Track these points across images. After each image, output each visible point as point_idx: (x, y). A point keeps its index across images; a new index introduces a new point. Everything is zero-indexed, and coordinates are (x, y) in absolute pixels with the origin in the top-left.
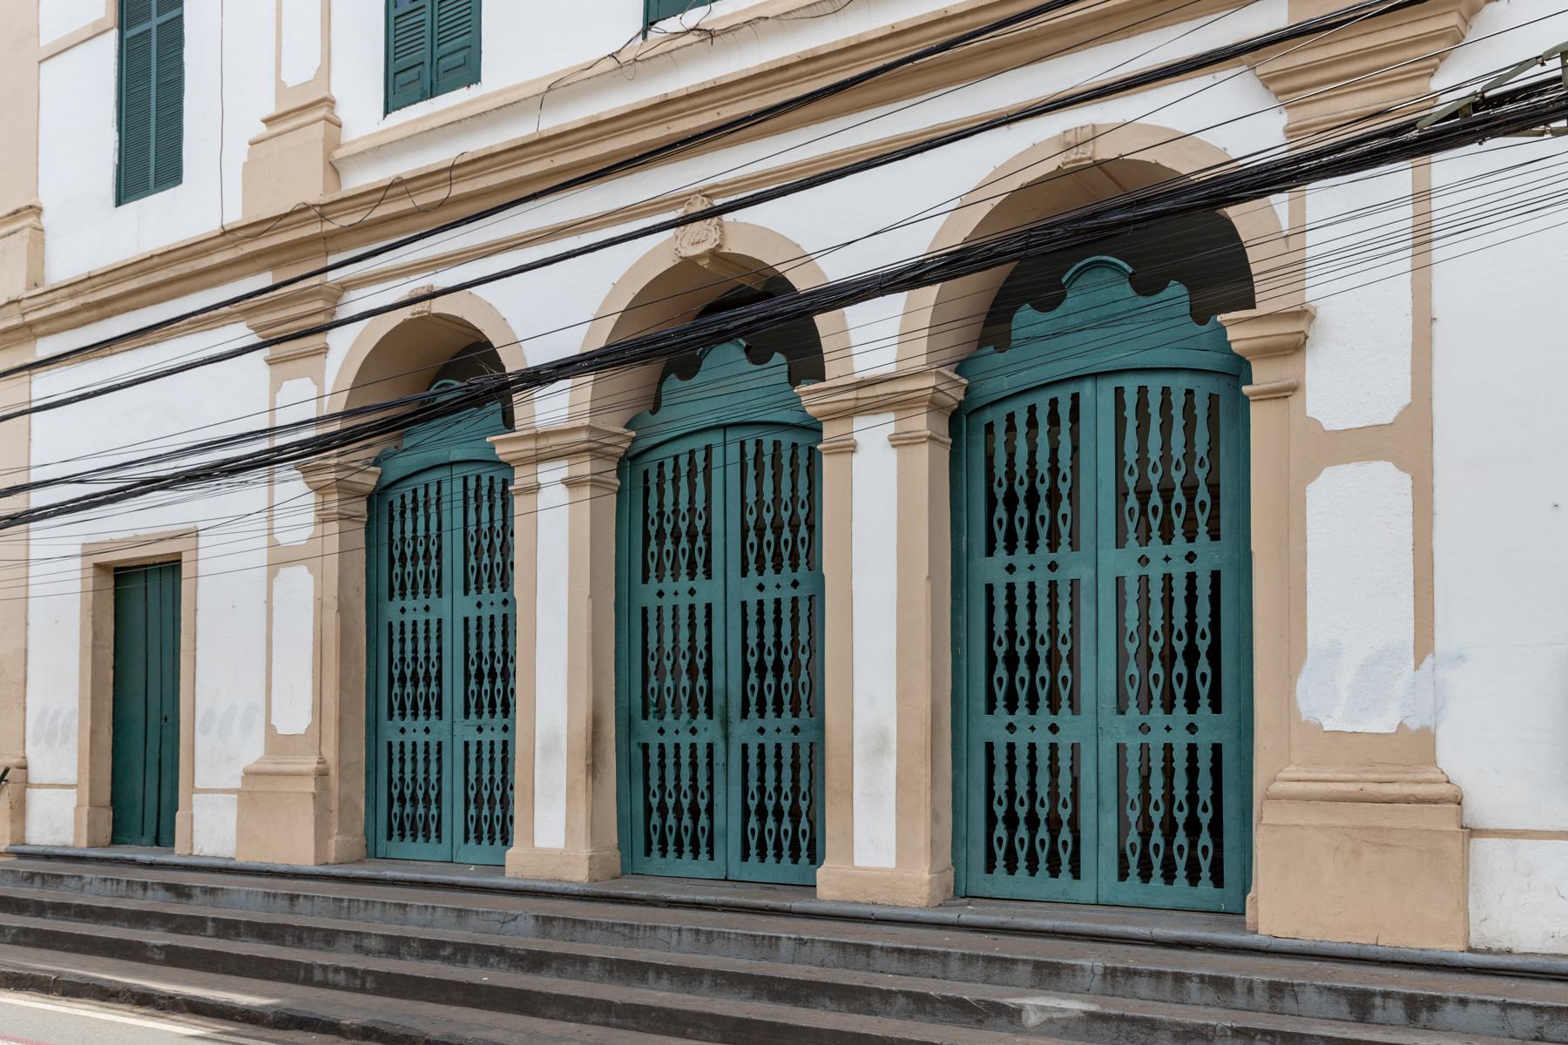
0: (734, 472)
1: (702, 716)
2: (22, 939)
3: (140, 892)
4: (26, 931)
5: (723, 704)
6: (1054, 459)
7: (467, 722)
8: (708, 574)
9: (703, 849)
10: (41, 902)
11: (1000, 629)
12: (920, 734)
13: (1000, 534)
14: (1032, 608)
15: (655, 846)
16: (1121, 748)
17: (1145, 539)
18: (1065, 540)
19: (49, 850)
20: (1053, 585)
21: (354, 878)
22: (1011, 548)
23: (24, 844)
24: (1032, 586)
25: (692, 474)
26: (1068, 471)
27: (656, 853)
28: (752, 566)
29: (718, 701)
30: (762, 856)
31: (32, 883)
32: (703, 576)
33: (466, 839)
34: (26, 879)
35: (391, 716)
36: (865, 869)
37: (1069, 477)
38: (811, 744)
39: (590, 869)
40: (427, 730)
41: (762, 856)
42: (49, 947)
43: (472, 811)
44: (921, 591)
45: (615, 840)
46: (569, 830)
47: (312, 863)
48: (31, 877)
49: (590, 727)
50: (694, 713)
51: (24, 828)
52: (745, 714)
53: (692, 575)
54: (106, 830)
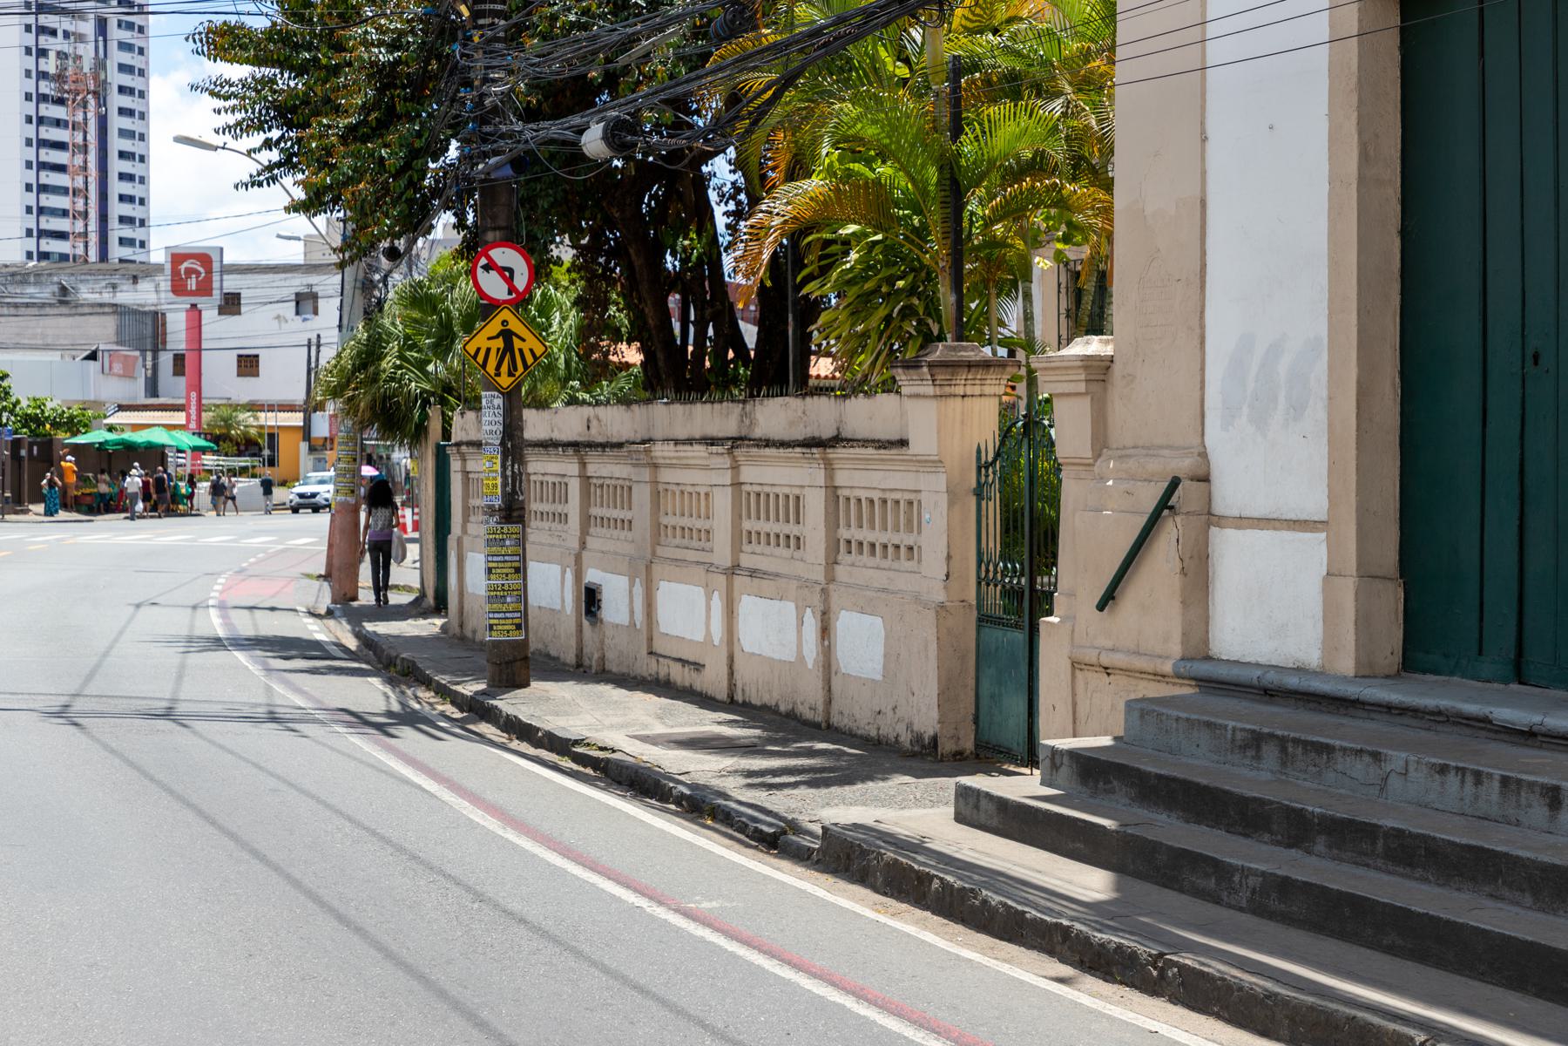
2: (1274, 904)
3: (1538, 812)
4: (1285, 886)
10: (1300, 813)
19: (1272, 678)
23: (1208, 658)
31: (1258, 757)
34: (1244, 747)
42: (1343, 935)
48: (1255, 742)
51: (1206, 620)
54: (1392, 637)
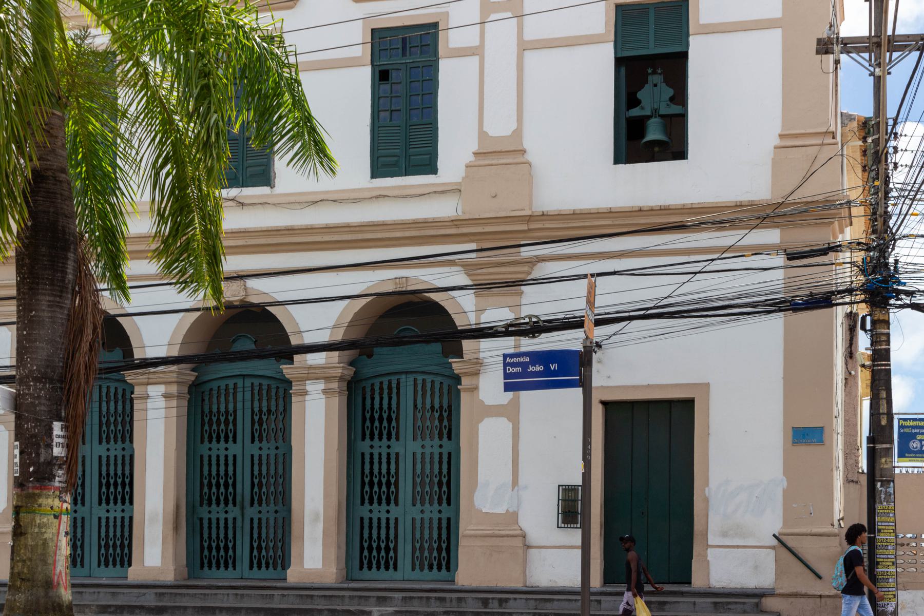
0: (248, 395)
1: (230, 505)
5: (241, 500)
6: (390, 404)
7: (100, 507)
8: (235, 441)
9: (230, 565)
11: (367, 471)
12: (333, 513)
13: (368, 433)
14: (380, 463)
15: (206, 565)
16: (414, 519)
17: (423, 439)
18: (394, 436)
20: (389, 454)
22: (372, 439)
24: (380, 454)
25: (227, 395)
26: (395, 409)
27: (206, 568)
28: (257, 439)
29: (239, 498)
30: (259, 567)
32: (232, 442)
33: (99, 565)
36: (308, 569)
37: (396, 411)
38: (284, 518)
39: (175, 575)
41: (259, 567)
43: (103, 551)
44: (334, 455)
45: (185, 562)
46: (163, 557)
49: (175, 510)
50: (226, 504)
52: (252, 504)
53: (226, 441)
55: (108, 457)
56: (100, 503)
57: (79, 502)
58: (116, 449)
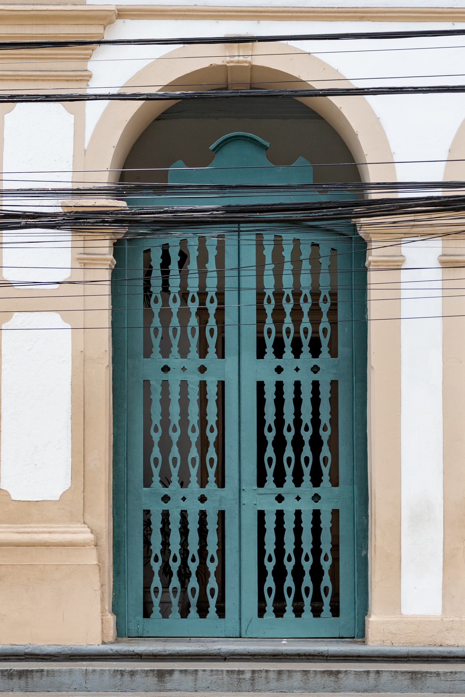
7: (261, 490)
21: (171, 655)
33: (261, 612)
35: (147, 482)
40: (203, 499)
47: (100, 642)
55: (279, 385)
56: (261, 482)
57: (212, 478)
58: (297, 369)
